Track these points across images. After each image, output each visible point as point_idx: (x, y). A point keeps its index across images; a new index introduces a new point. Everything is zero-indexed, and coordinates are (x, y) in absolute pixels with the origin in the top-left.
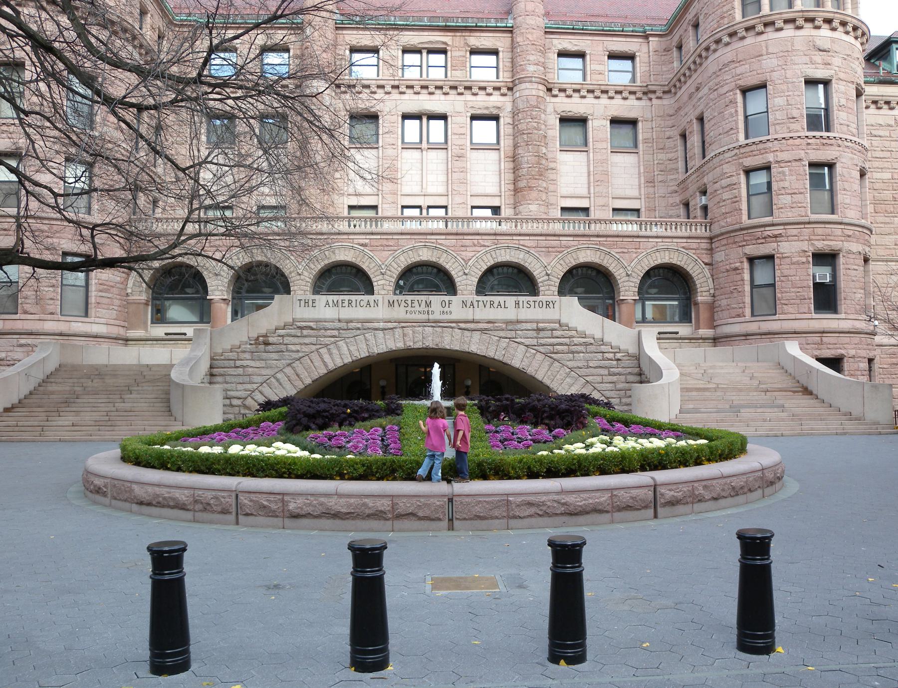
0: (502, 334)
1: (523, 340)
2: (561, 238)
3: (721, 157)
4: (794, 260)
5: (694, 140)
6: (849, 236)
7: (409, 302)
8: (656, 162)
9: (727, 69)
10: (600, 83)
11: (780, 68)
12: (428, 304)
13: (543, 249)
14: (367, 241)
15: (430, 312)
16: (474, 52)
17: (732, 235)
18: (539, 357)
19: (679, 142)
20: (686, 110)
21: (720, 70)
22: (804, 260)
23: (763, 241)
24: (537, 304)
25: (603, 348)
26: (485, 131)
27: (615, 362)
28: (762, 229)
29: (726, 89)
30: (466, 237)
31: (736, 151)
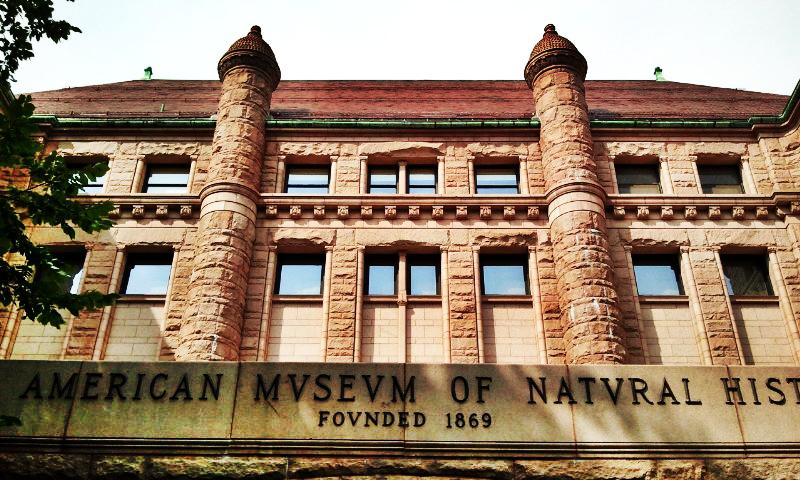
15: (411, 420)
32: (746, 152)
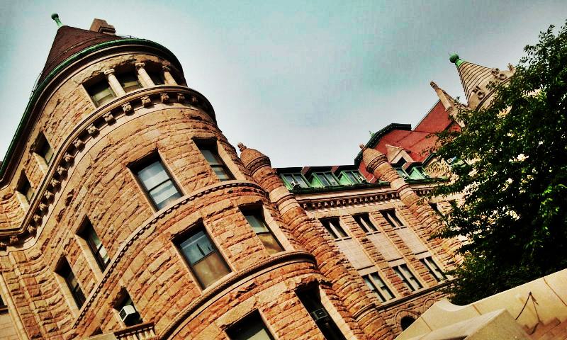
3: (136, 243)
9: (104, 156)
11: (165, 136)
17: (193, 316)
19: (60, 281)
21: (96, 160)
23: (236, 301)
29: (112, 174)
31: (153, 226)
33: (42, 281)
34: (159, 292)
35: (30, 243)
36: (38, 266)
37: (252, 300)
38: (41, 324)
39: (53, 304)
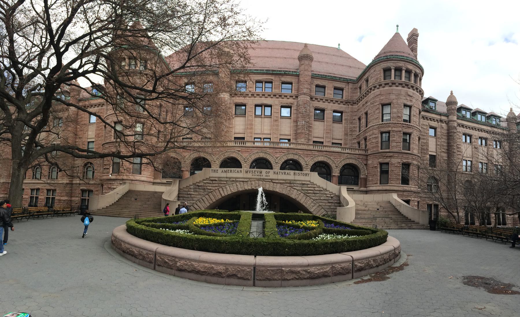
0: (288, 185)
1: (296, 188)
2: (312, 152)
3: (373, 127)
4: (396, 165)
5: (363, 121)
6: (414, 159)
7: (254, 172)
8: (349, 127)
10: (330, 97)
12: (261, 173)
13: (306, 155)
14: (240, 149)
16: (283, 83)
17: (375, 155)
18: (302, 194)
19: (358, 121)
20: (362, 110)
22: (399, 165)
23: (385, 158)
24: (302, 174)
25: (326, 192)
26: (285, 112)
27: (330, 198)
28: (386, 153)
30: (277, 149)
31: (378, 126)
32: (345, 87)
33: (354, 119)
34: (372, 144)
35: (355, 106)
36: (355, 114)
37: (389, 159)
38: (349, 131)
39: (354, 127)
